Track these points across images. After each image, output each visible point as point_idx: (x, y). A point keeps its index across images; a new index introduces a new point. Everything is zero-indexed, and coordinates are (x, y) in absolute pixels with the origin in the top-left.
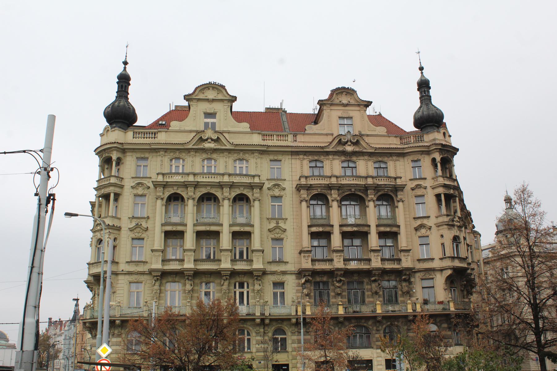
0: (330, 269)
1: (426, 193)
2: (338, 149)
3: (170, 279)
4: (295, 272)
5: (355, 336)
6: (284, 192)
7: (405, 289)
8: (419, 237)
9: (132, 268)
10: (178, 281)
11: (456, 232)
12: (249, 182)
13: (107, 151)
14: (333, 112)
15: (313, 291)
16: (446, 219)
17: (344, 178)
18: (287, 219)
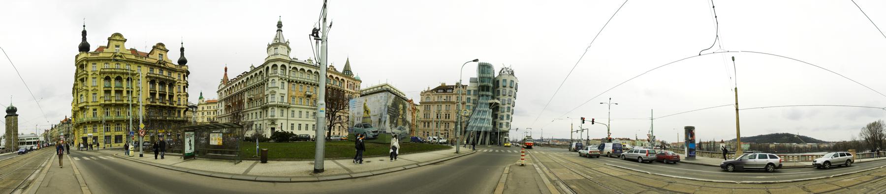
9: (93, 104)
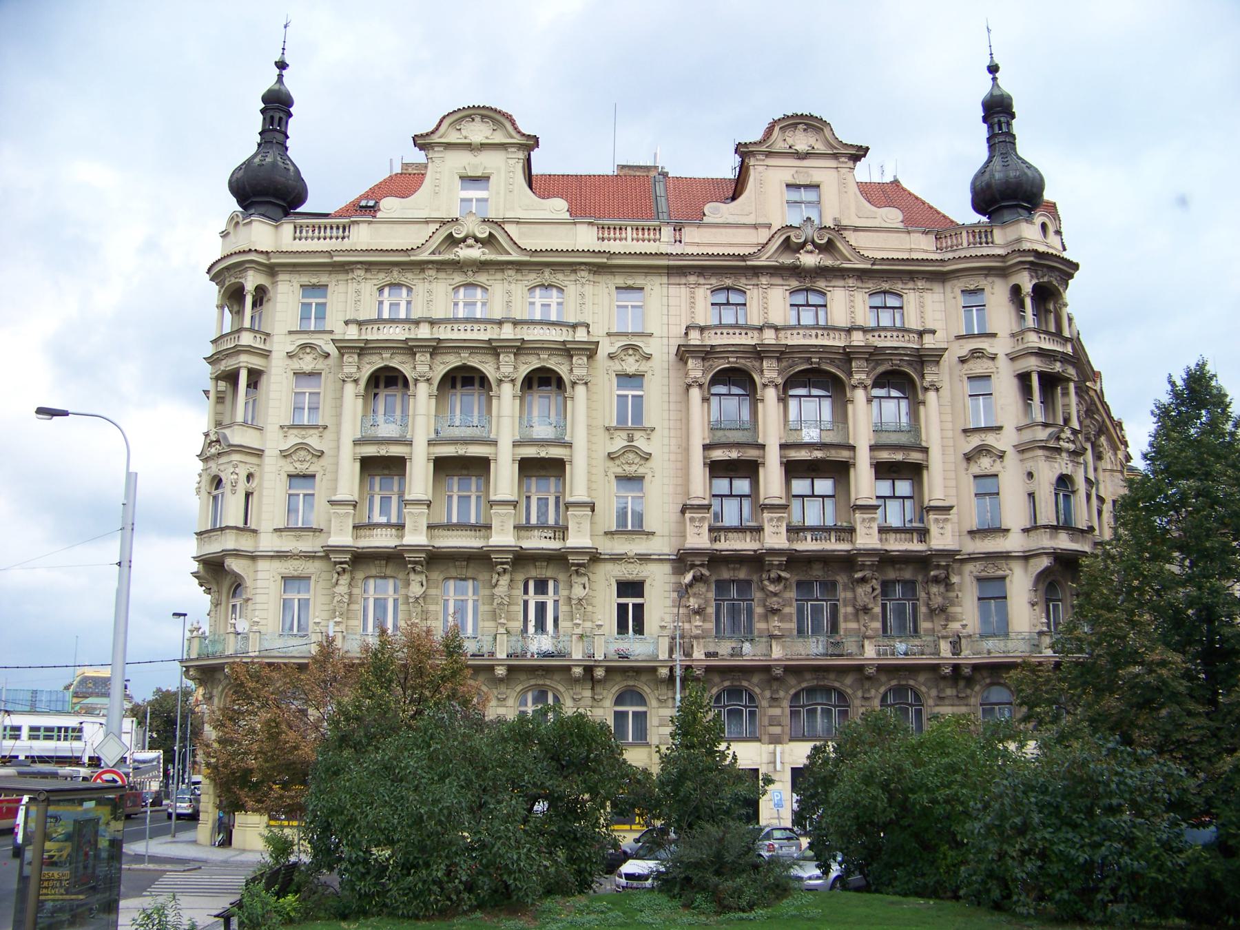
0: (755, 551)
1: (994, 370)
2: (781, 261)
3: (374, 572)
4: (671, 557)
5: (812, 713)
6: (649, 363)
7: (937, 601)
8: (975, 477)
9: (288, 544)
10: (393, 574)
11: (1063, 465)
12: (561, 339)
13: (232, 271)
14: (771, 171)
15: (713, 603)
16: (1042, 434)
17: (795, 332)
18: (653, 430)
